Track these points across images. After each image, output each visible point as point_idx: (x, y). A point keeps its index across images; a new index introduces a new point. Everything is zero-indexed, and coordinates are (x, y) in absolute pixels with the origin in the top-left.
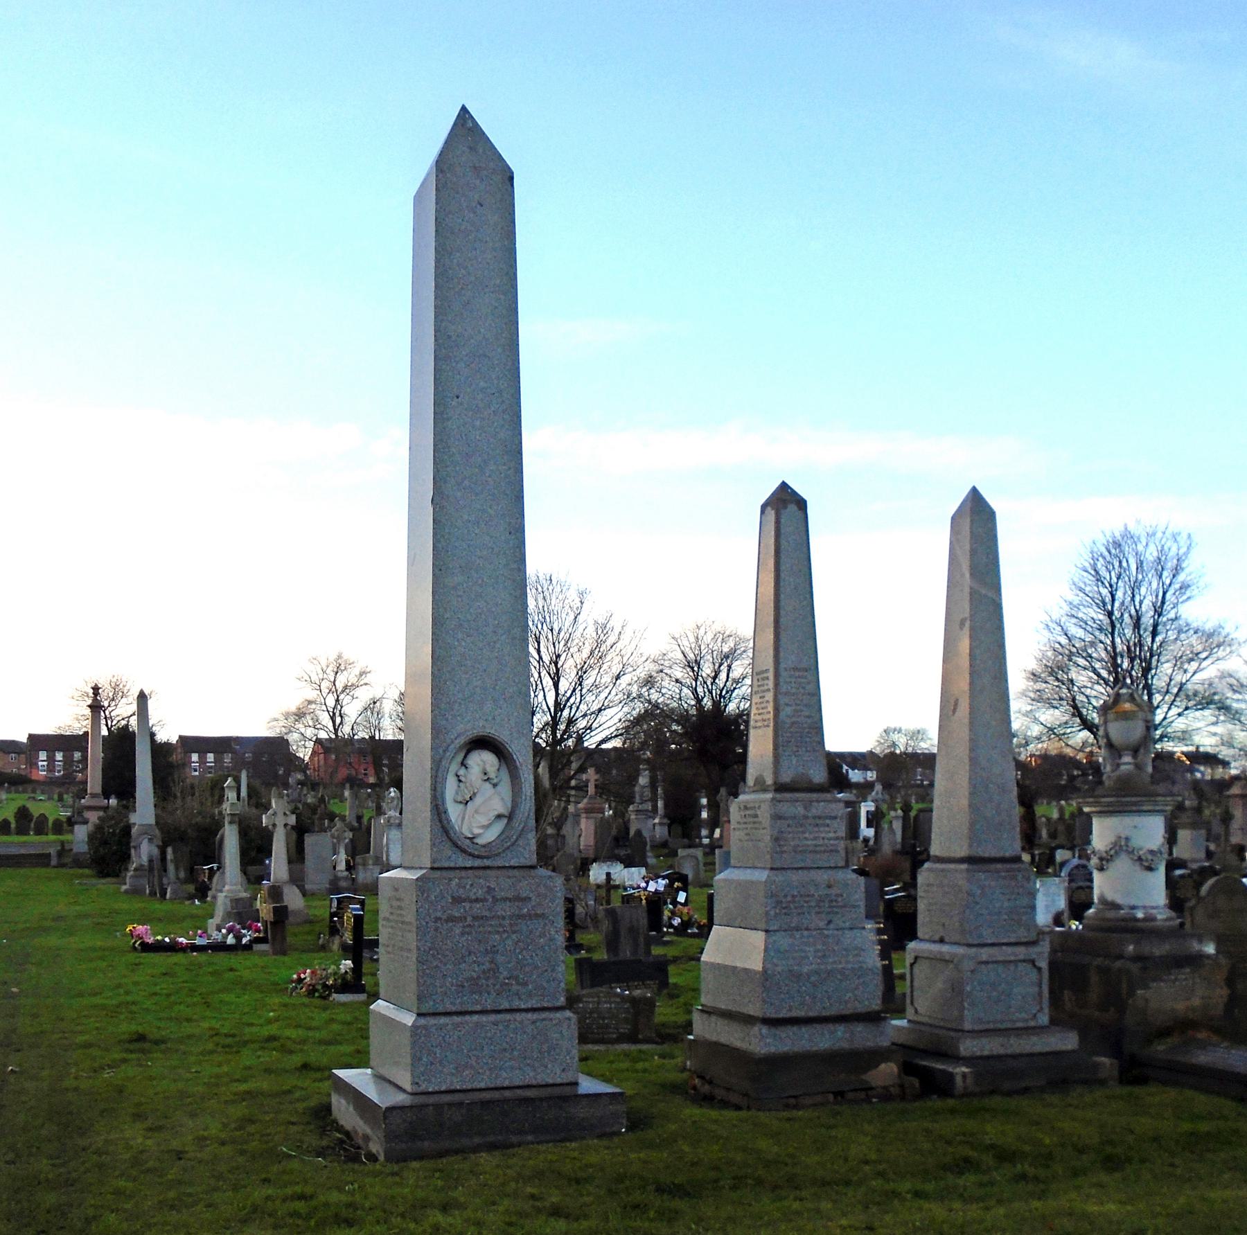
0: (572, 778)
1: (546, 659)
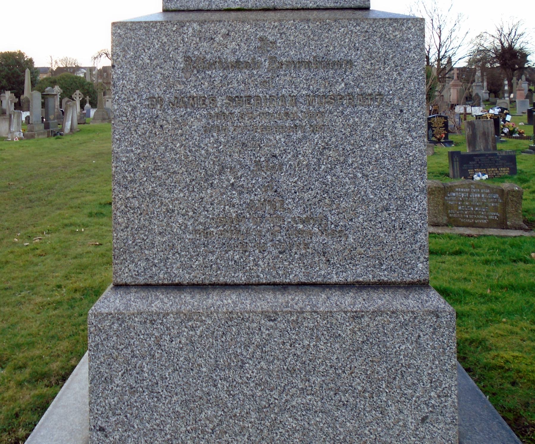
0: (447, 74)
1: (436, 27)
